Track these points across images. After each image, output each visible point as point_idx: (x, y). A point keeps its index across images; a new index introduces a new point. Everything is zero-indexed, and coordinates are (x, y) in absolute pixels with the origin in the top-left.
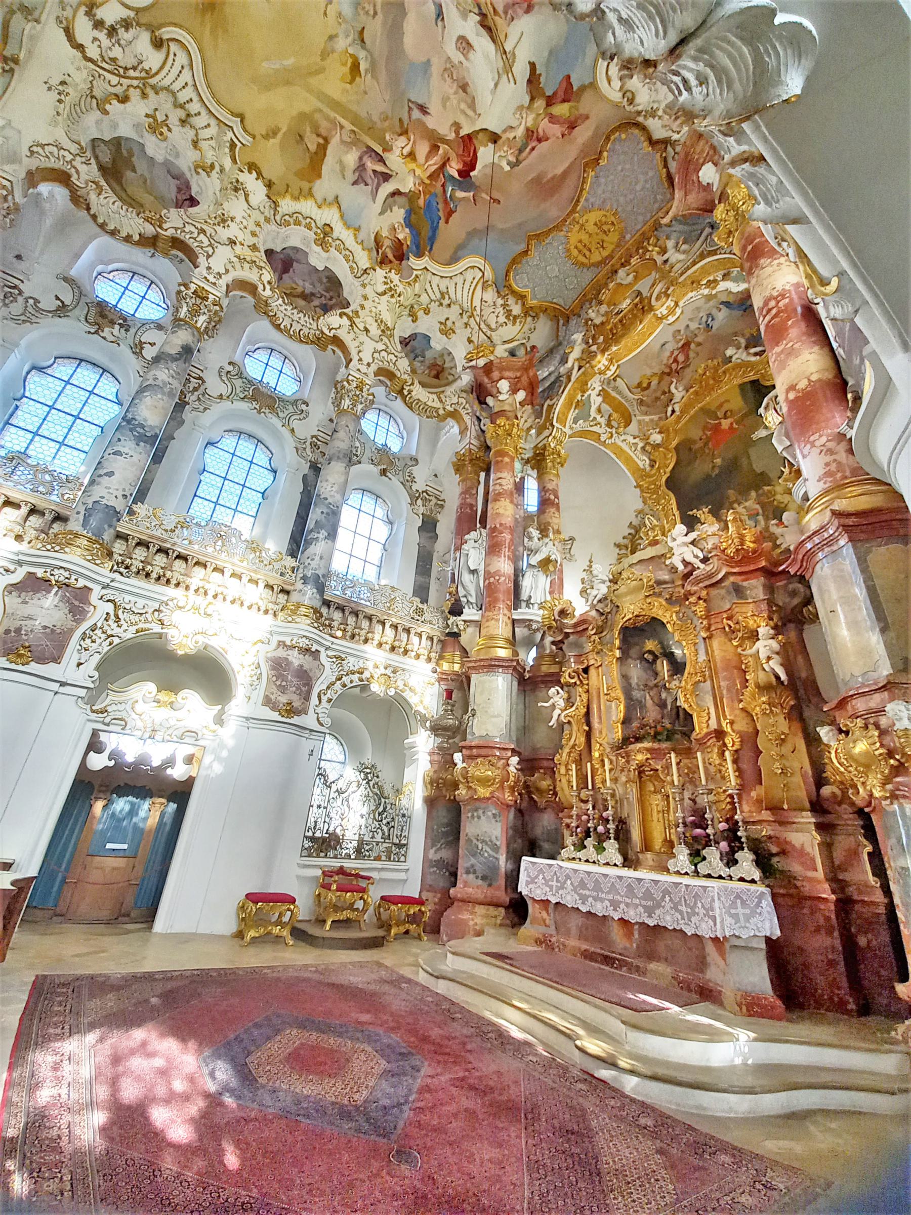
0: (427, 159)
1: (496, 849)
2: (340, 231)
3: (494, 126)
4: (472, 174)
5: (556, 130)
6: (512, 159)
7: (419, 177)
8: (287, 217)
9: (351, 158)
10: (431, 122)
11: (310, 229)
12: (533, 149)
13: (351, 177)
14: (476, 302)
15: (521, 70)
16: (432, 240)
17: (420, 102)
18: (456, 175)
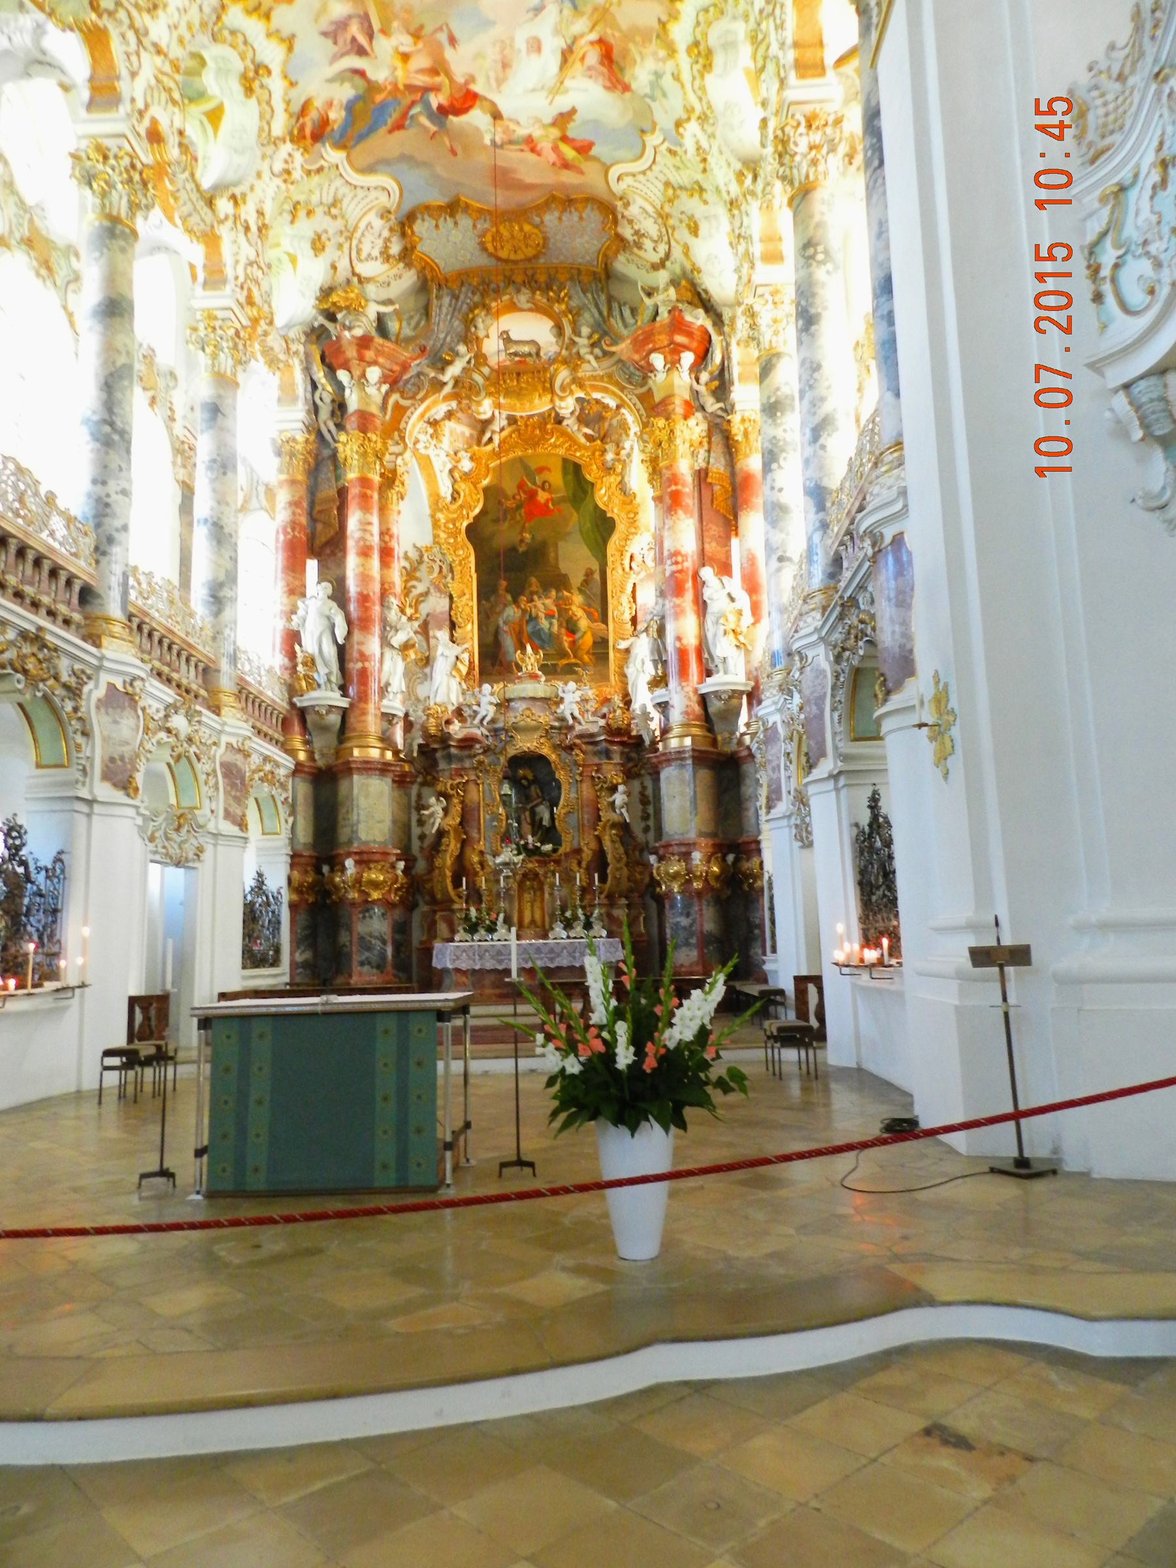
0: (422, 71)
1: (384, 942)
2: (276, 84)
3: (504, 107)
4: (451, 117)
5: (552, 157)
6: (498, 140)
7: (396, 78)
8: (226, 33)
9: (339, 10)
10: (449, 53)
11: (243, 58)
12: (522, 150)
13: (324, 24)
14: (362, 225)
15: (563, 103)
16: (361, 138)
17: (457, 34)
18: (435, 105)
